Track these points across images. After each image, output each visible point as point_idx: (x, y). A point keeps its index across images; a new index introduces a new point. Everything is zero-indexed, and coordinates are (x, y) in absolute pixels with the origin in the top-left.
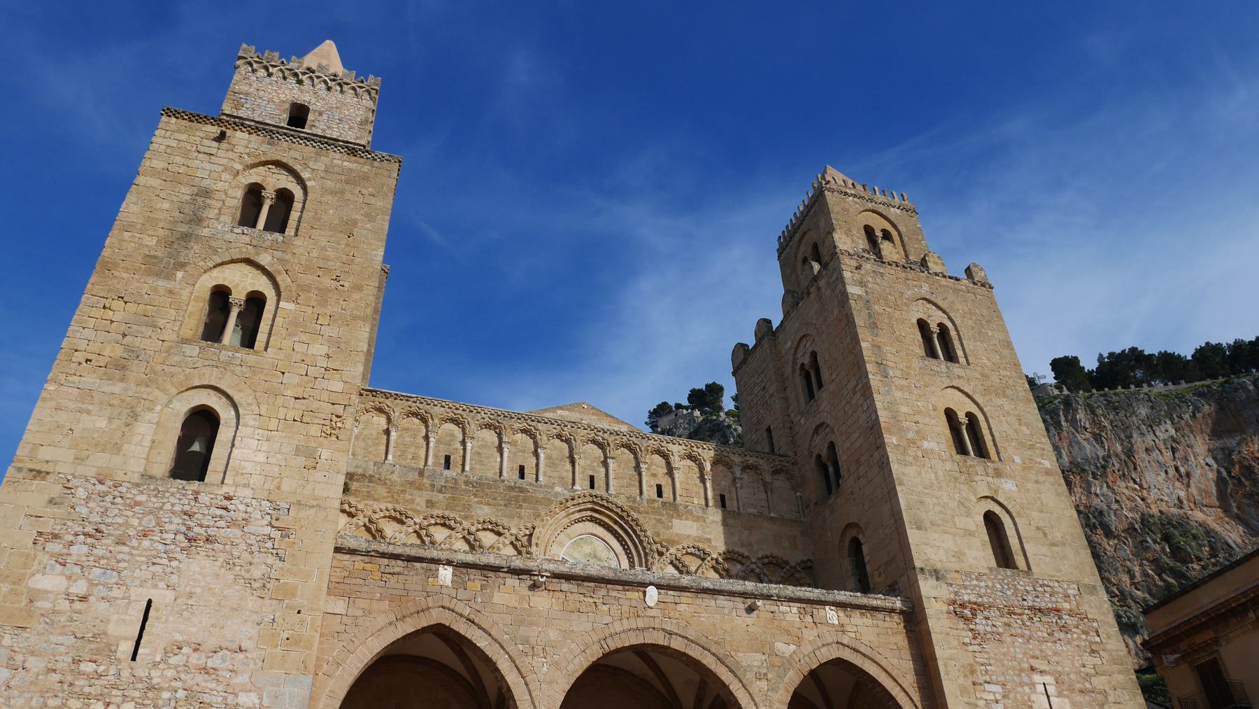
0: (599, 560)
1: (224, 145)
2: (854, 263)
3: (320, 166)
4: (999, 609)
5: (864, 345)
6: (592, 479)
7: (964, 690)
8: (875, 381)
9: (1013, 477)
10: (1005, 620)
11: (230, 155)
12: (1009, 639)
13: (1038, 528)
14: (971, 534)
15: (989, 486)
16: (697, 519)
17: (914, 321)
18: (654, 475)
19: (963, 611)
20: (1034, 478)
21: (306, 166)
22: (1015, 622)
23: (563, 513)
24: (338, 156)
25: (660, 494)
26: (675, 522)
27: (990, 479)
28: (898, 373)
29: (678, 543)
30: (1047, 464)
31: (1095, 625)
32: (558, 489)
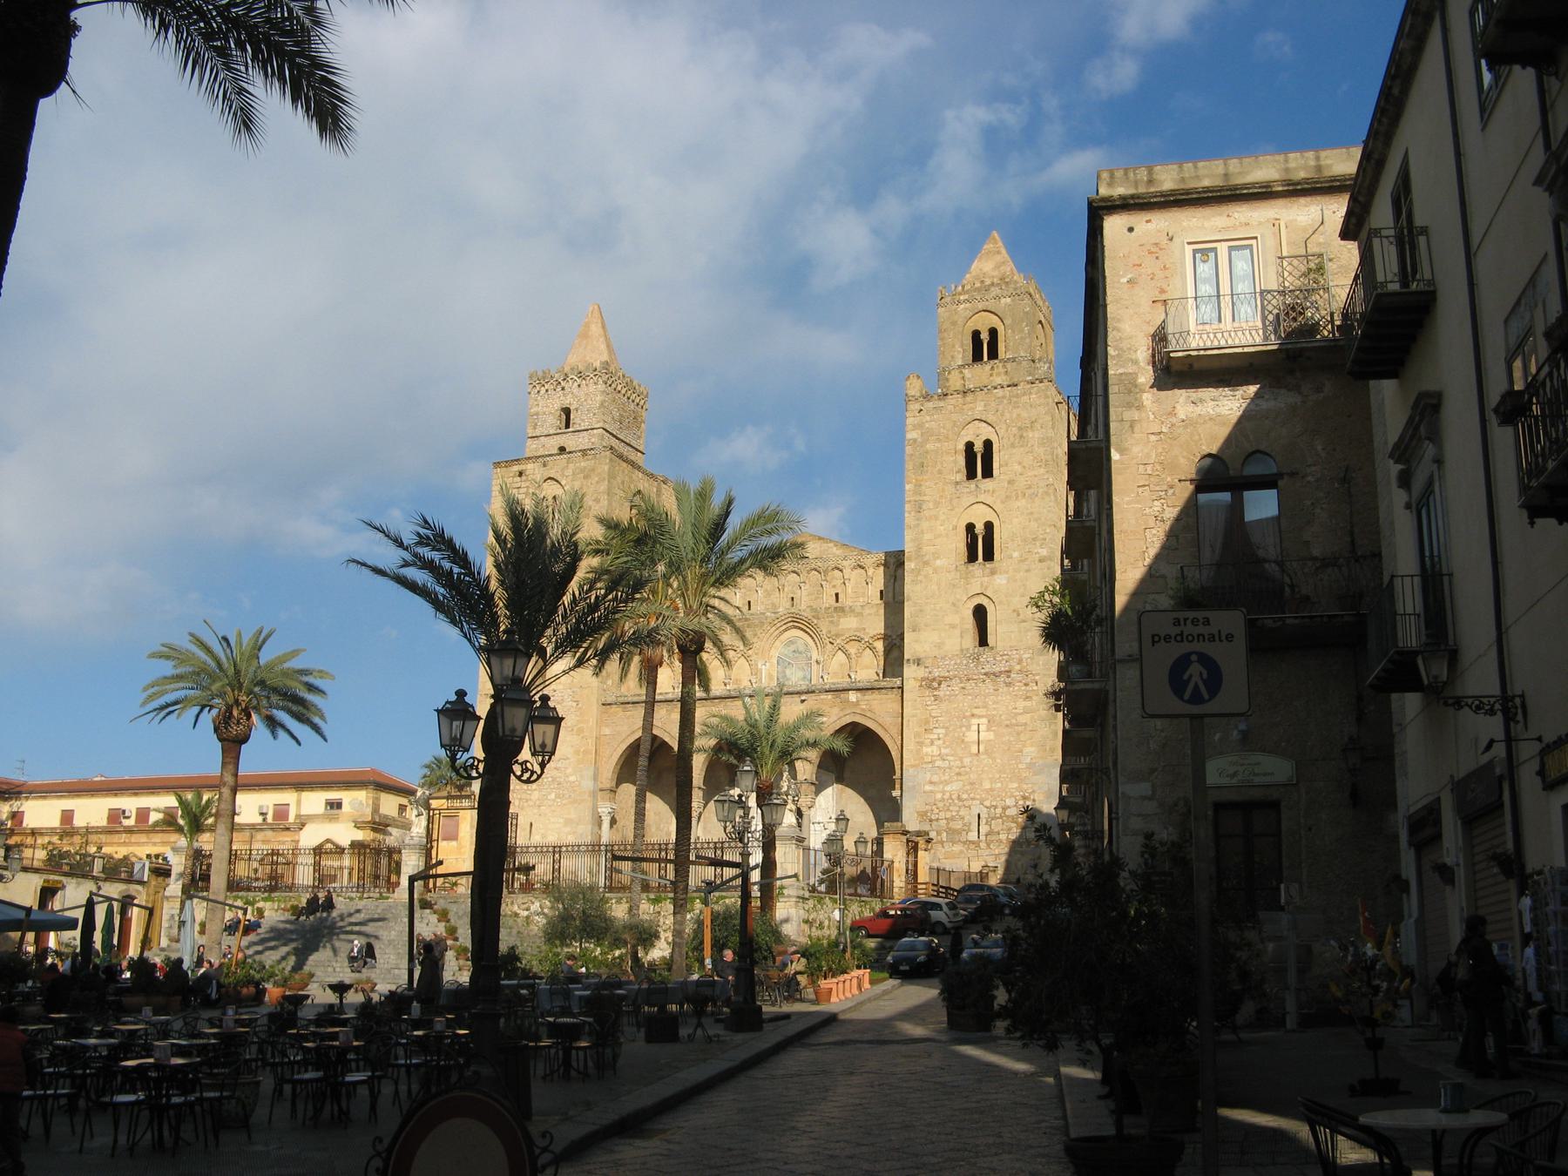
0: (800, 653)
1: (524, 478)
2: (918, 406)
3: (569, 472)
4: (960, 678)
5: (908, 487)
6: (793, 599)
7: (917, 735)
8: (909, 518)
9: (1007, 572)
10: (962, 685)
11: (528, 484)
12: (960, 697)
13: (1014, 611)
14: (953, 626)
15: (982, 585)
16: (860, 615)
17: (961, 446)
18: (834, 586)
19: (931, 684)
20: (1026, 567)
21: (563, 475)
22: (968, 686)
23: (774, 628)
24: (577, 460)
25: (837, 601)
26: (841, 620)
27: (986, 579)
28: (931, 505)
29: (843, 635)
30: (1044, 552)
31: (1037, 678)
32: (769, 614)
